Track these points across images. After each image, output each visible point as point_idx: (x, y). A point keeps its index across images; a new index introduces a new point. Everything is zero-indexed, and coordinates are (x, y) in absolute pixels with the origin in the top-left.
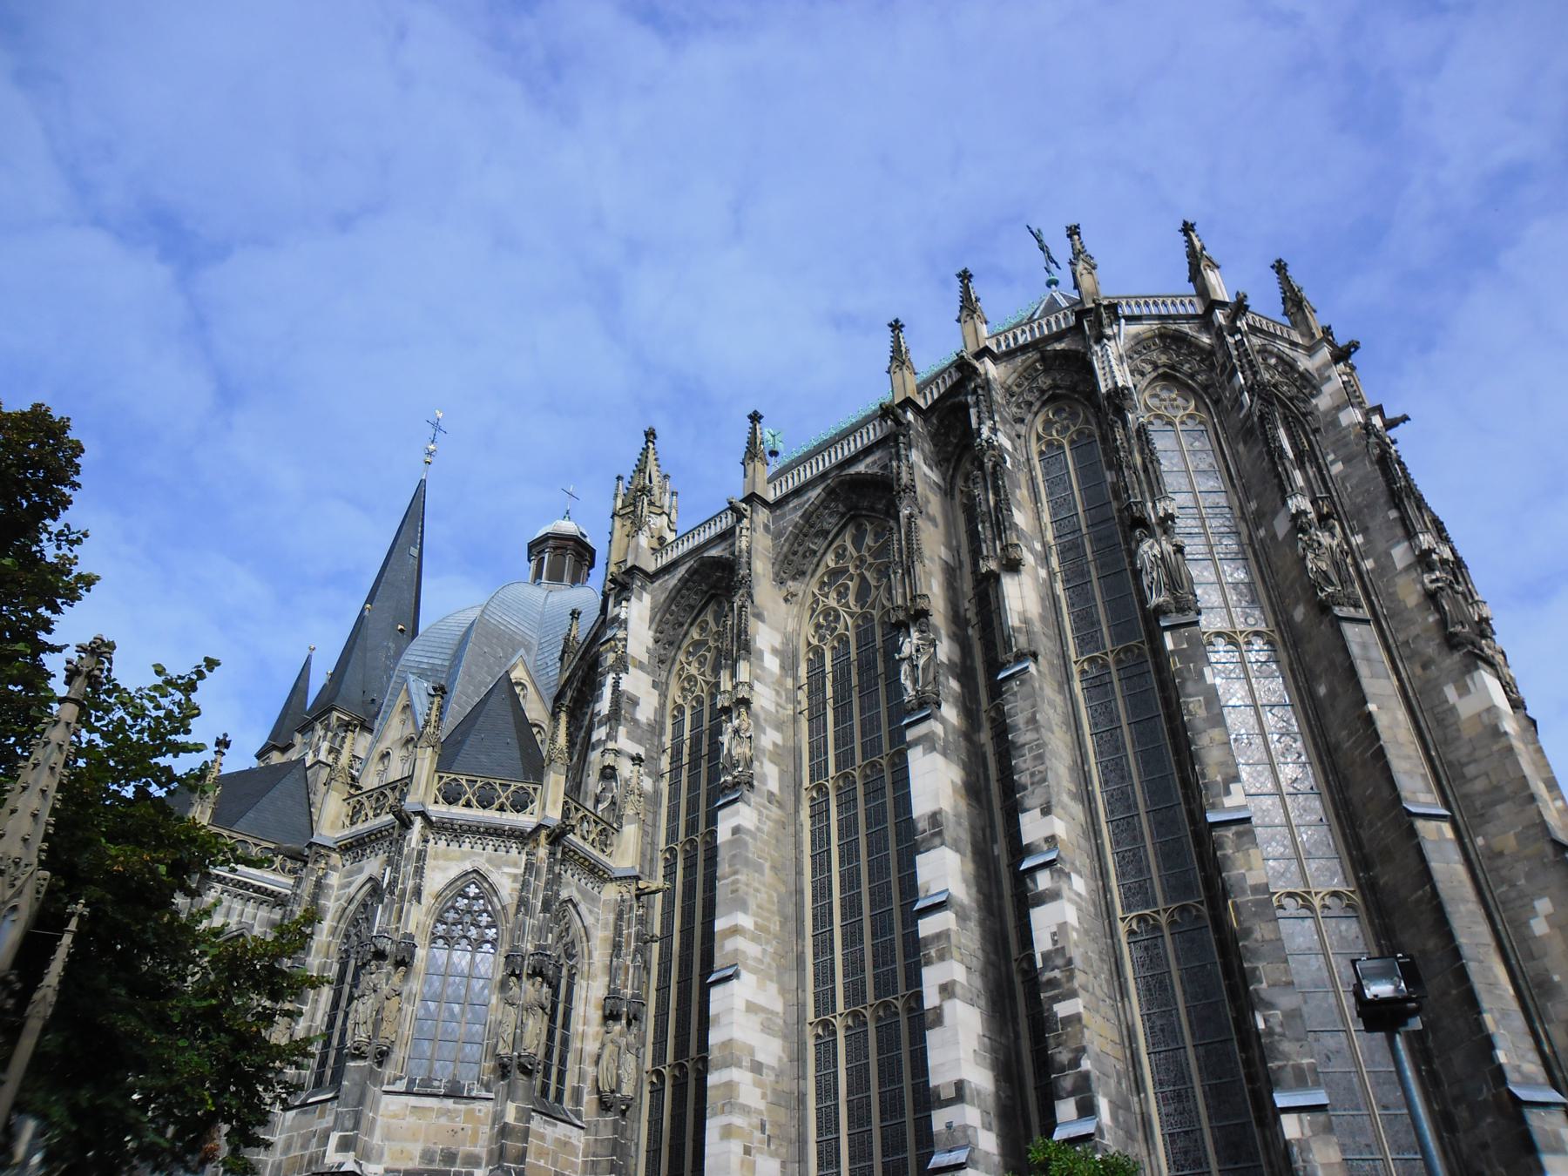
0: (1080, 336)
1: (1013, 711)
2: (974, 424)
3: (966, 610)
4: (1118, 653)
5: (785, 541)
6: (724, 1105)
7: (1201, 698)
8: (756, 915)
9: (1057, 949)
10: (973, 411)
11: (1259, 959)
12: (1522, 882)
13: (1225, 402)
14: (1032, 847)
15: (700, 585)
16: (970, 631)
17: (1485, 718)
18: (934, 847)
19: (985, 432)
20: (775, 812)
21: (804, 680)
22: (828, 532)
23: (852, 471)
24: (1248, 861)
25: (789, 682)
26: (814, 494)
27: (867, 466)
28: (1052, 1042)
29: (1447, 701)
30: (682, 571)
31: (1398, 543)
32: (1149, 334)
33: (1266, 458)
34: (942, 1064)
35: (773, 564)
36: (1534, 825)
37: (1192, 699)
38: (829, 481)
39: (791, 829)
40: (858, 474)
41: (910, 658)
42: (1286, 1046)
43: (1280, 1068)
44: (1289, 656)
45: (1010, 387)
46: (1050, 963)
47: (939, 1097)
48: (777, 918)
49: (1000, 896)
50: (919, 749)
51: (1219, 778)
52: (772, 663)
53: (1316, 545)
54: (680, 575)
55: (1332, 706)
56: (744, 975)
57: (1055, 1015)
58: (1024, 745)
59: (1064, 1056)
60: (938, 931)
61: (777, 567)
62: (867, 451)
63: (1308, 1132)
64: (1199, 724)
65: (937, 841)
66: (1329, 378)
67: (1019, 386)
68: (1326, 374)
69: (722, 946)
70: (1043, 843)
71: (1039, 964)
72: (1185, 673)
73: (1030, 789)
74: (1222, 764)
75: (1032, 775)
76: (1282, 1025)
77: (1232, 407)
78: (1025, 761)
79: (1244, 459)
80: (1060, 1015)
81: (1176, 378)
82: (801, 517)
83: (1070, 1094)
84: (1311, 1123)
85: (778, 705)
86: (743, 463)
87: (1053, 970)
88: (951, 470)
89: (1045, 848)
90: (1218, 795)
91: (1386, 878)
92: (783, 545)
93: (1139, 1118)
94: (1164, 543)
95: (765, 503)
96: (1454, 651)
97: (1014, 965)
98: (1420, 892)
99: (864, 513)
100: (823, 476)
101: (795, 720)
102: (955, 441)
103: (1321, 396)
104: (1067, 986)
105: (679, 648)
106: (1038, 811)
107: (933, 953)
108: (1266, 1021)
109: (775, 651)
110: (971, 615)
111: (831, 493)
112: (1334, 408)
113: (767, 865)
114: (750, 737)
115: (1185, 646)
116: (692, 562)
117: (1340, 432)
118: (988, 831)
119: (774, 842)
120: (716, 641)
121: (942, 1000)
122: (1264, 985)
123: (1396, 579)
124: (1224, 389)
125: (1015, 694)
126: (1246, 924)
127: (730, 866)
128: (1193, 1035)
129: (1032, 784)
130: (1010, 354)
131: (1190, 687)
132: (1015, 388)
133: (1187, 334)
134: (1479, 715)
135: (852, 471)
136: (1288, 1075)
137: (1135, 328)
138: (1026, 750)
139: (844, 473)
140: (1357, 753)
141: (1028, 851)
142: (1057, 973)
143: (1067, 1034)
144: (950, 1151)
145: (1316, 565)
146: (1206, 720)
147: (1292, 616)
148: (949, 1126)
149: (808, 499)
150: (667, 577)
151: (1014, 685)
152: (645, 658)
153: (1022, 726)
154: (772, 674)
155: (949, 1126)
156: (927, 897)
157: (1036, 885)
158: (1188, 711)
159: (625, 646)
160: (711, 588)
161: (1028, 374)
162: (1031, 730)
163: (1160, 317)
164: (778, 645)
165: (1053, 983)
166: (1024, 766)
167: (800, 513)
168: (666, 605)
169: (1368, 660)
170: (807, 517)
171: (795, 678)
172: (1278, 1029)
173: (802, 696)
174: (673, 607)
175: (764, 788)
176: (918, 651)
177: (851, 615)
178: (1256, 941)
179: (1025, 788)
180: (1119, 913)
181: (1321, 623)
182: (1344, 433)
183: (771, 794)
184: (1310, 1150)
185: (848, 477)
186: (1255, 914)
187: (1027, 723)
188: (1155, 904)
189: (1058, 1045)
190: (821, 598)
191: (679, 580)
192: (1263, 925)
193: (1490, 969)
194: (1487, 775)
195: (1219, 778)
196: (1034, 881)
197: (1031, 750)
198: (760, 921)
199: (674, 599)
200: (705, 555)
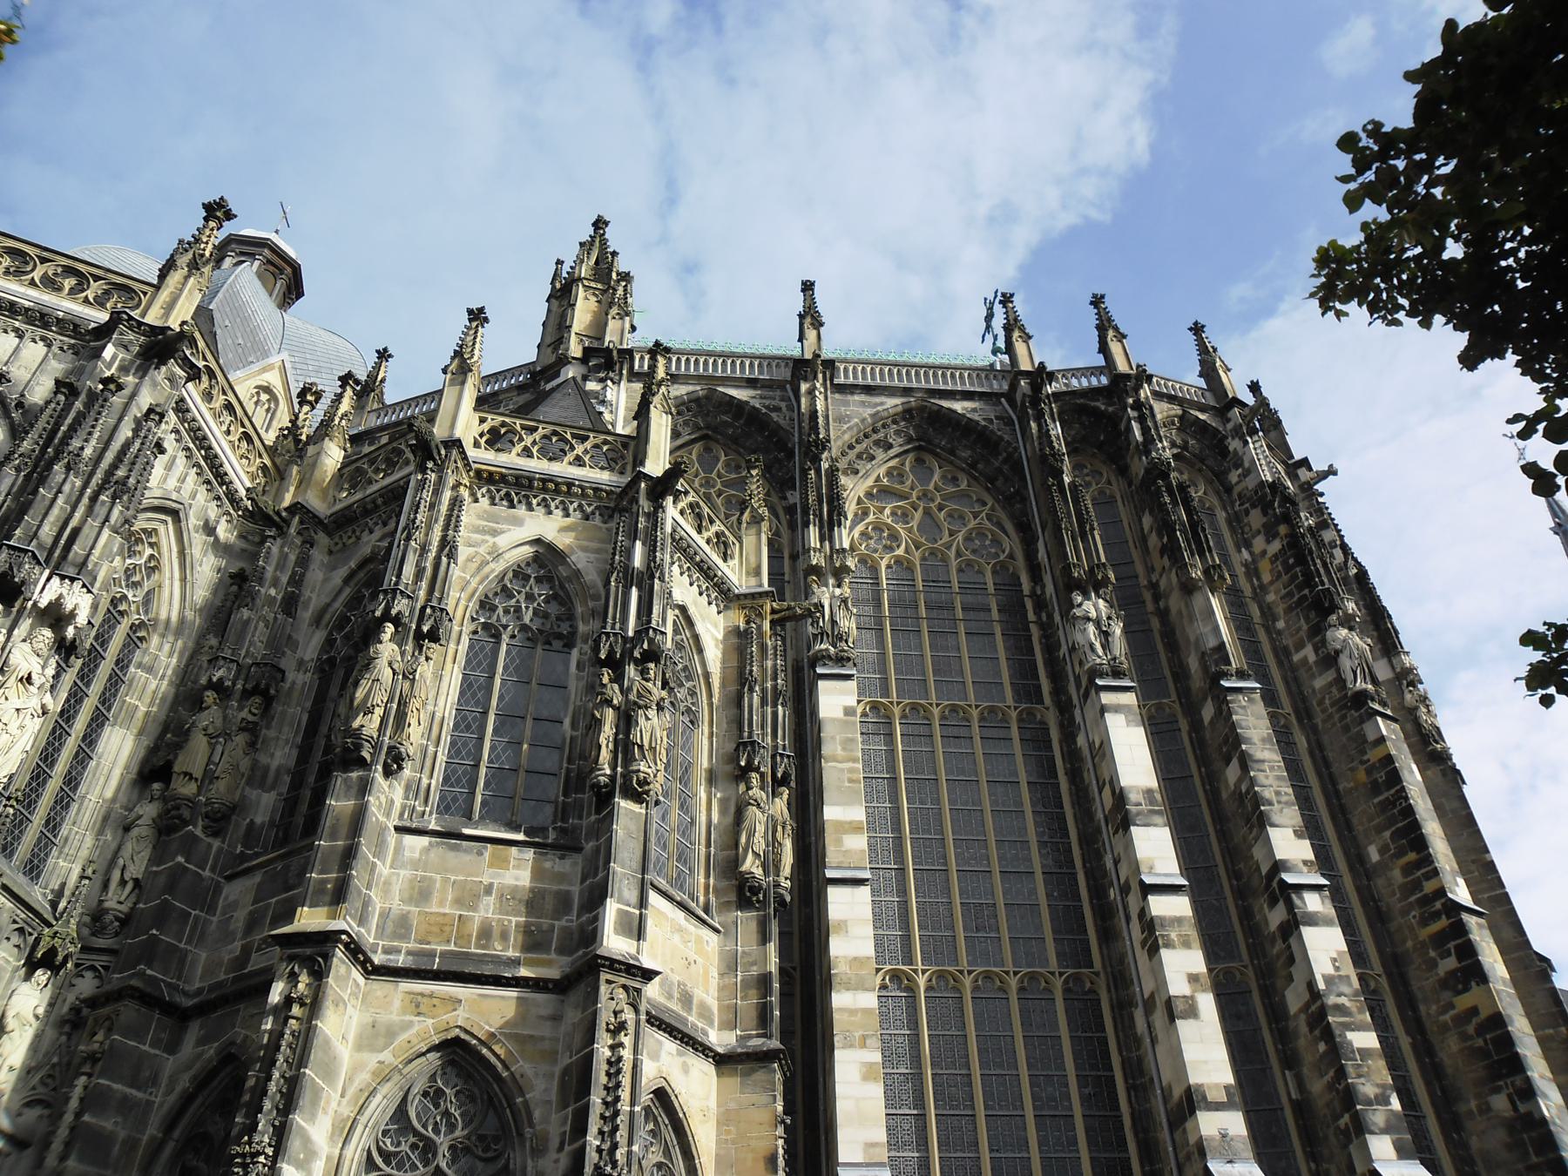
6: (864, 1037)
18: (1155, 825)
22: (890, 446)
23: (945, 404)
28: (1350, 1071)
34: (1206, 1062)
40: (954, 412)
46: (1335, 988)
69: (839, 842)
70: (1301, 865)
78: (1267, 777)
87: (1339, 995)
92: (845, 432)
100: (907, 391)
111: (907, 414)
116: (698, 388)
121: (1194, 991)
135: (945, 404)
149: (882, 404)
160: (708, 427)
185: (936, 408)
189: (1359, 1076)
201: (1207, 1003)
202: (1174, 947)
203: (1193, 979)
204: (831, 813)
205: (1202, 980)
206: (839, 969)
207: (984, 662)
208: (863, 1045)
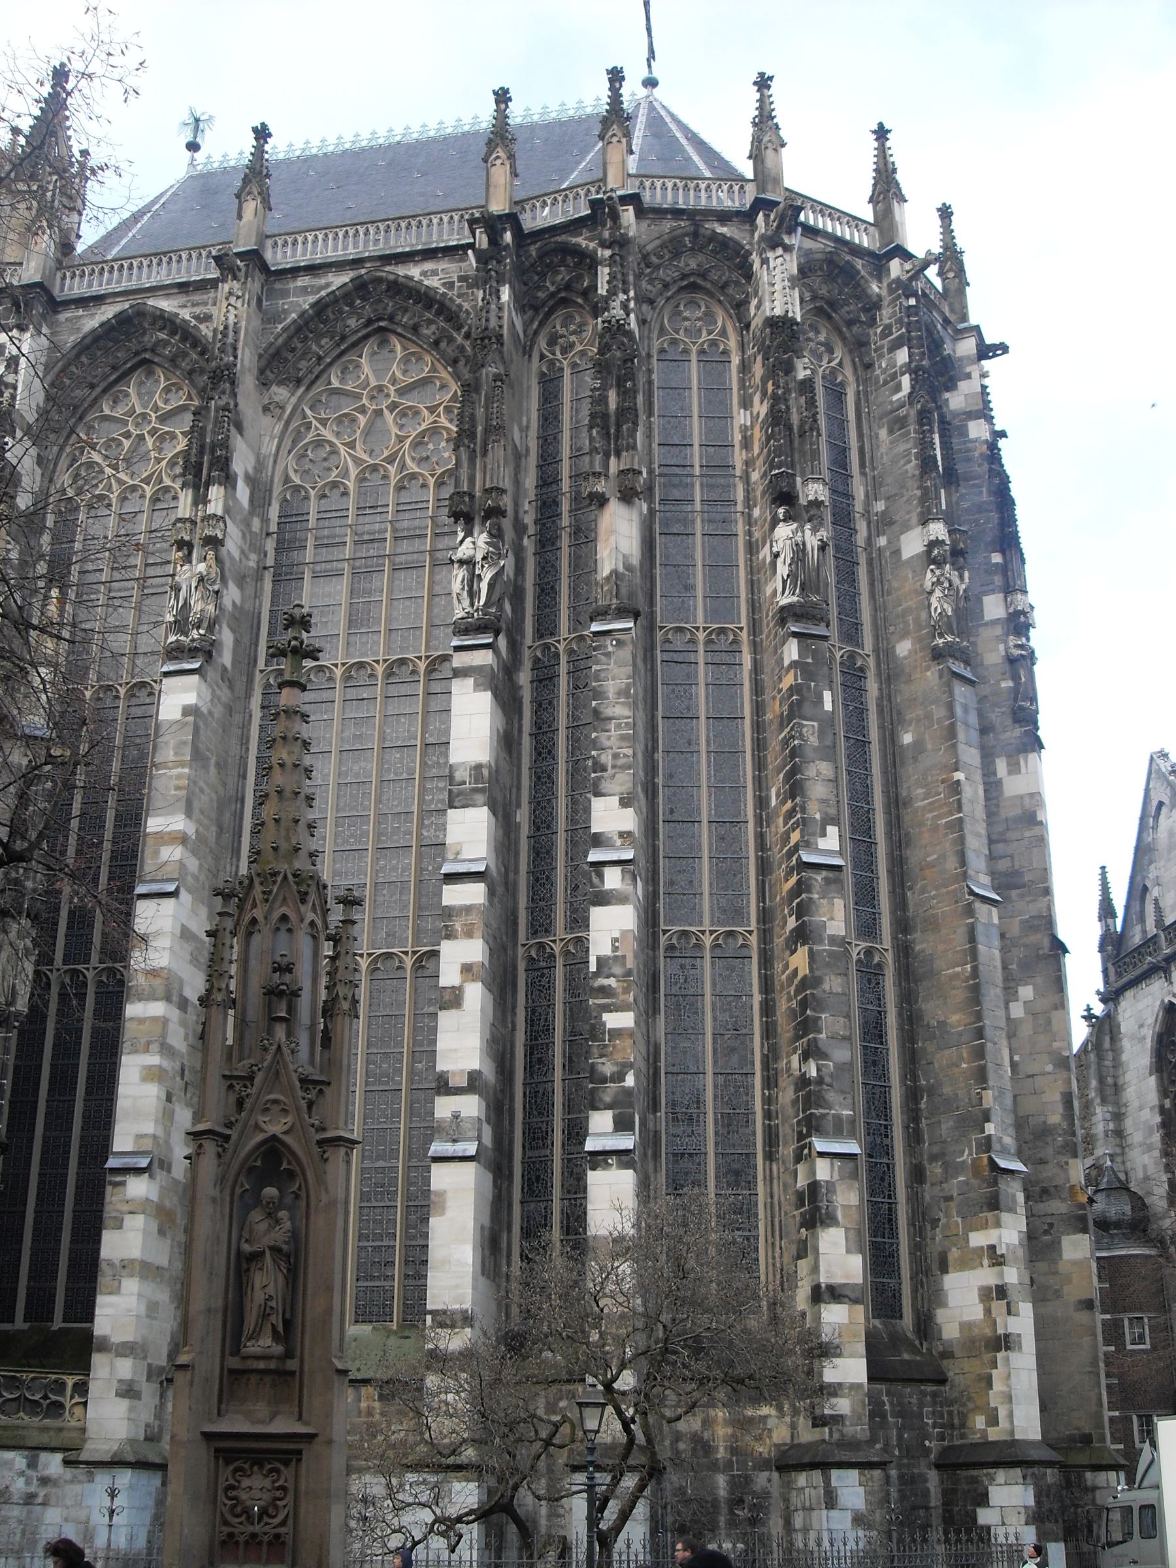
0: (747, 227)
1: (602, 675)
2: (602, 290)
3: (526, 512)
4: (710, 633)
5: (284, 330)
6: (148, 1043)
7: (815, 724)
8: (199, 822)
9: (616, 957)
10: (604, 273)
11: (823, 1011)
12: (1014, 967)
13: (878, 372)
14: (604, 838)
15: (129, 341)
16: (526, 541)
17: (1027, 801)
18: (474, 806)
19: (617, 312)
20: (225, 694)
21: (273, 528)
22: (343, 338)
23: (401, 271)
24: (832, 911)
25: (256, 523)
26: (338, 280)
27: (424, 274)
29: (995, 774)
30: (108, 312)
31: (993, 592)
32: (819, 256)
33: (914, 462)
34: (456, 1050)
35: (260, 356)
36: (1040, 917)
37: (805, 722)
38: (363, 271)
39: (238, 718)
40: (411, 278)
41: (468, 563)
42: (831, 1096)
43: (824, 1116)
44: (880, 689)
45: (648, 254)
47: (447, 1083)
48: (214, 829)
49: (516, 872)
50: (470, 681)
51: (818, 816)
52: (243, 492)
53: (946, 584)
54: (104, 318)
55: (915, 759)
56: (185, 896)
57: (604, 1024)
58: (610, 719)
59: (608, 1069)
60: (468, 902)
61: (264, 362)
62: (430, 254)
63: (836, 1177)
64: (809, 753)
65: (480, 798)
66: (968, 376)
67: (661, 257)
68: (968, 370)
69: (157, 853)
70: (616, 837)
71: (593, 967)
72: (805, 690)
73: (610, 771)
74: (822, 801)
75: (616, 756)
76: (831, 1076)
77: (886, 383)
78: (609, 738)
79: (883, 450)
80: (608, 1026)
81: (829, 317)
82: (313, 306)
83: (609, 1107)
84: (840, 1168)
85: (242, 552)
86: (238, 196)
87: (608, 977)
88: (536, 324)
89: (619, 842)
90: (814, 834)
91: (924, 946)
93: (651, 1134)
94: (808, 533)
95: (264, 267)
96: (1017, 725)
97: (521, 951)
98: (959, 969)
99: (399, 330)
100: (357, 262)
101: (259, 578)
102: (552, 289)
103: (955, 393)
104: (622, 997)
105: (81, 418)
106: (617, 798)
107: (458, 927)
108: (818, 1070)
109: (249, 479)
110: (529, 519)
111: (360, 288)
112: (965, 413)
113: (213, 761)
114: (217, 592)
115: (810, 660)
117: (965, 443)
118: (514, 790)
119: (220, 731)
120: (137, 425)
121: (464, 981)
122: (823, 1036)
123: (981, 630)
124: (881, 356)
125: (608, 655)
126: (817, 973)
127: (176, 754)
128: (715, 1062)
129: (614, 767)
130: (659, 213)
131: (807, 709)
132: (654, 259)
133: (858, 272)
134: (1021, 797)
135: (401, 271)
136: (829, 1125)
137: (809, 244)
138: (612, 725)
139: (388, 268)
140: (930, 816)
141: (598, 841)
142: (612, 982)
143: (614, 1046)
144: (455, 1141)
145: (942, 606)
146: (816, 749)
147: (894, 647)
148: (456, 1116)
149: (328, 285)
150: (81, 312)
151: (610, 644)
152: (31, 417)
153: (611, 696)
154: (242, 509)
155: (456, 1116)
156: (456, 860)
157: (602, 881)
158: (801, 734)
159: (13, 397)
161: (673, 247)
162: (622, 703)
163: (840, 241)
164: (251, 471)
165: (605, 991)
166: (607, 743)
167: (312, 299)
168: (75, 352)
169: (966, 724)
170: (320, 307)
171: (265, 521)
172: (827, 1080)
173: (270, 545)
174: (84, 359)
175: (219, 660)
176: (484, 558)
177: (357, 461)
178: (824, 991)
179: (604, 769)
180: (662, 927)
181: (928, 668)
182: (970, 445)
183: (225, 669)
184: (835, 1192)
185: (392, 277)
186: (828, 965)
187: (619, 694)
188: (701, 923)
189: (601, 1056)
190: (314, 422)
191: (102, 325)
192: (833, 977)
193: (1000, 1049)
194: (1012, 857)
195: (818, 816)
196: (601, 876)
197: (618, 727)
198: (201, 829)
199: (87, 348)
200: (151, 302)
201: (475, 995)
202: (456, 938)
203: (467, 969)
204: (154, 824)
205: (475, 969)
206: (139, 981)
207: (407, 603)
208: (147, 1051)
